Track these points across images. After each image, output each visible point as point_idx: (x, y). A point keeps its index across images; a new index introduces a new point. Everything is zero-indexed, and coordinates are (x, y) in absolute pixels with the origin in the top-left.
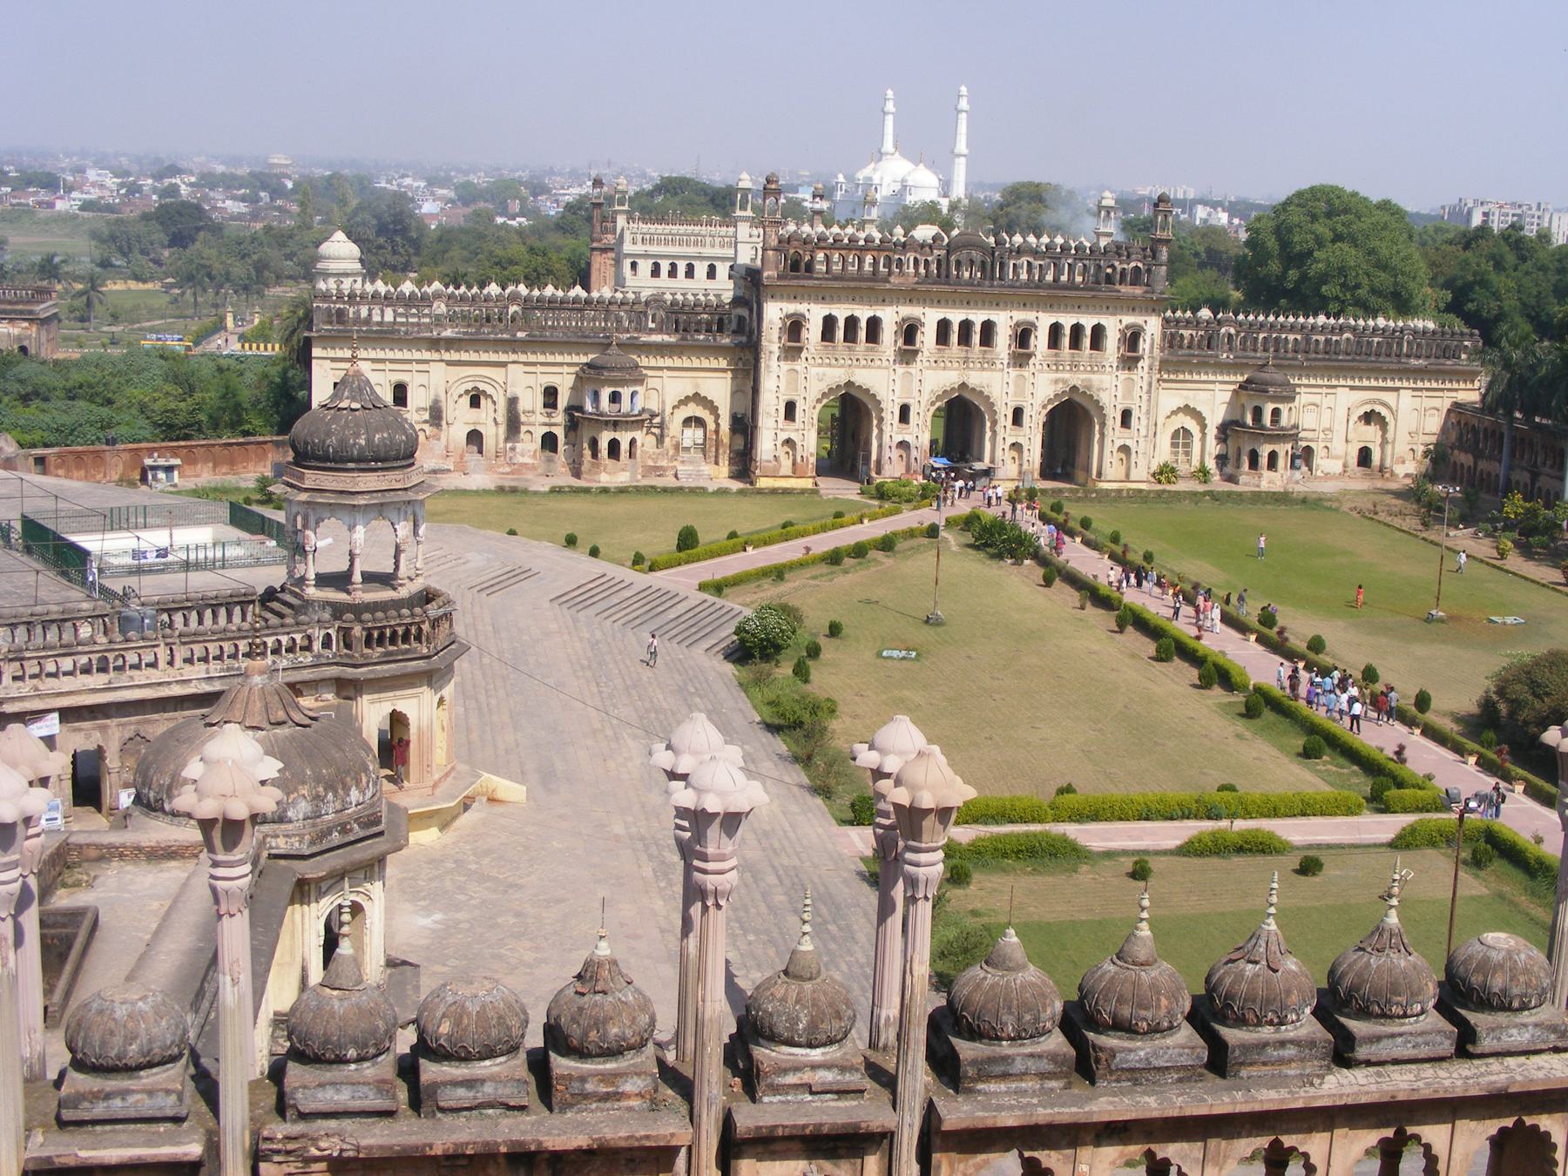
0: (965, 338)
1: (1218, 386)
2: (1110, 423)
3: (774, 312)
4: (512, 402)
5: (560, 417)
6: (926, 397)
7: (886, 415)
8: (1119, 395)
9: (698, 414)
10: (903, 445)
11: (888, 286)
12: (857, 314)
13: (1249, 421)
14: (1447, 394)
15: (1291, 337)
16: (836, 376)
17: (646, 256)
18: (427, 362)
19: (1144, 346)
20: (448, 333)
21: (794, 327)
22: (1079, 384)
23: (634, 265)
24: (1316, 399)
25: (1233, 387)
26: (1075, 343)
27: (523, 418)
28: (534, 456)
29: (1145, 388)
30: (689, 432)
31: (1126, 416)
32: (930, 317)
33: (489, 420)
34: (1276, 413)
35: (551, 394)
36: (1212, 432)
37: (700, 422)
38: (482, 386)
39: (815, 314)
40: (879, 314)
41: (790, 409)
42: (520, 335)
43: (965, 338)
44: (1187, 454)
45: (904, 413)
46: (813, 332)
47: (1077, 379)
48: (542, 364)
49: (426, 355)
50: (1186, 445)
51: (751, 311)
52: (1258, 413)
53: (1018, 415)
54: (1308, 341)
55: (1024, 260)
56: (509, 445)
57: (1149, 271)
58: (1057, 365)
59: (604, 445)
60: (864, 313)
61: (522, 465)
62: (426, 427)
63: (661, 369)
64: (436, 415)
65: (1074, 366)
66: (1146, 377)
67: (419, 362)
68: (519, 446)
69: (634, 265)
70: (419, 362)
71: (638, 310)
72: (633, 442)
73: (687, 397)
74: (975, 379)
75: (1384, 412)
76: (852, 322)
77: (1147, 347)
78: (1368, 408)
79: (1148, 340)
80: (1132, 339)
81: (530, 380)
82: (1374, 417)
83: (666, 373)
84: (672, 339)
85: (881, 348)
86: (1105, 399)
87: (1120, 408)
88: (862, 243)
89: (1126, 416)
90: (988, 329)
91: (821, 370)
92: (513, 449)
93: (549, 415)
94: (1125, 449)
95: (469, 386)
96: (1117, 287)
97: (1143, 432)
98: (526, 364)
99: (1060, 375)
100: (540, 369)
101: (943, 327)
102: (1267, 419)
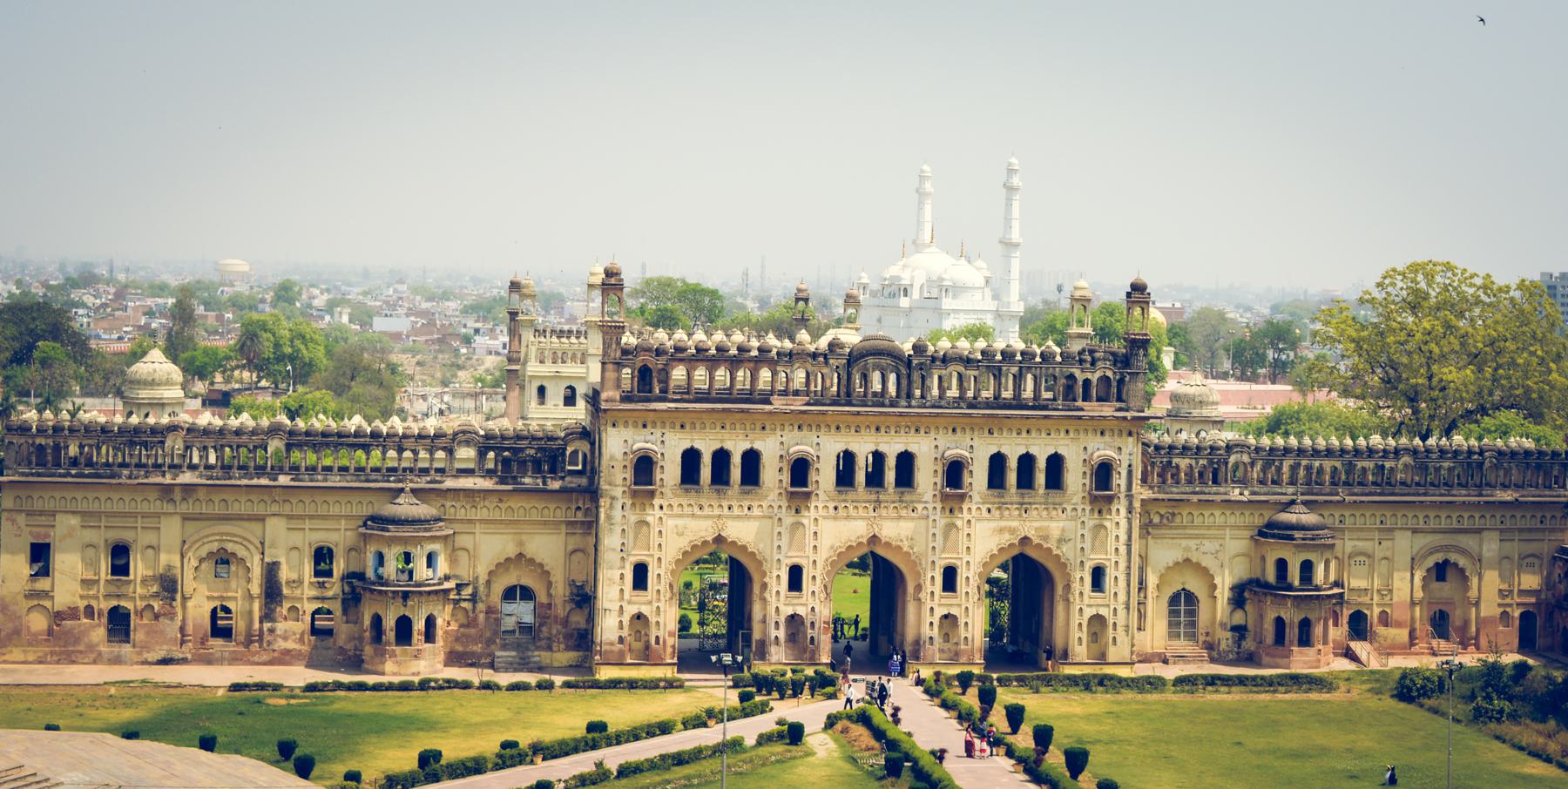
0: (875, 479)
2: (1076, 586)
3: (618, 444)
4: (271, 571)
5: (334, 587)
6: (823, 555)
7: (771, 581)
8: (1087, 545)
9: (527, 581)
10: (794, 619)
11: (767, 407)
12: (728, 446)
13: (1271, 576)
14: (1547, 536)
15: (1328, 464)
17: (557, 377)
18: (158, 516)
19: (1119, 480)
20: (187, 477)
21: (644, 467)
22: (1031, 534)
23: (542, 391)
24: (1360, 544)
25: (1247, 534)
26: (1026, 480)
27: (285, 591)
28: (301, 640)
29: (1123, 538)
30: (509, 607)
31: (1098, 575)
32: (825, 449)
34: (1307, 567)
35: (323, 556)
36: (1223, 594)
37: (527, 594)
38: (230, 547)
39: (669, 448)
40: (757, 446)
41: (640, 576)
42: (283, 480)
43: (875, 479)
44: (1193, 624)
45: (795, 578)
48: (311, 517)
49: (157, 506)
50: (1192, 613)
51: (592, 444)
52: (1282, 565)
53: (950, 579)
54: (1350, 468)
55: (954, 370)
56: (267, 625)
57: (1121, 382)
59: (389, 623)
60: (737, 448)
61: (287, 652)
63: (470, 521)
64: (169, 586)
66: (1124, 524)
67: (145, 516)
68: (281, 626)
69: (542, 391)
70: (145, 516)
71: (445, 442)
72: (430, 622)
73: (508, 560)
75: (1462, 562)
76: (721, 457)
77: (1123, 482)
78: (1439, 557)
79: (1124, 473)
80: (1103, 474)
81: (297, 538)
82: (1450, 574)
83: (478, 528)
84: (487, 484)
85: (762, 491)
86: (1068, 552)
87: (1089, 566)
88: (754, 353)
89: (1098, 575)
90: (906, 462)
91: (680, 522)
92: (272, 631)
93: (321, 585)
94: (1098, 620)
95: (215, 547)
96: (1080, 403)
97: (1122, 597)
98: (290, 517)
99: (1003, 524)
100: (307, 524)
101: (847, 461)
102: (1294, 576)
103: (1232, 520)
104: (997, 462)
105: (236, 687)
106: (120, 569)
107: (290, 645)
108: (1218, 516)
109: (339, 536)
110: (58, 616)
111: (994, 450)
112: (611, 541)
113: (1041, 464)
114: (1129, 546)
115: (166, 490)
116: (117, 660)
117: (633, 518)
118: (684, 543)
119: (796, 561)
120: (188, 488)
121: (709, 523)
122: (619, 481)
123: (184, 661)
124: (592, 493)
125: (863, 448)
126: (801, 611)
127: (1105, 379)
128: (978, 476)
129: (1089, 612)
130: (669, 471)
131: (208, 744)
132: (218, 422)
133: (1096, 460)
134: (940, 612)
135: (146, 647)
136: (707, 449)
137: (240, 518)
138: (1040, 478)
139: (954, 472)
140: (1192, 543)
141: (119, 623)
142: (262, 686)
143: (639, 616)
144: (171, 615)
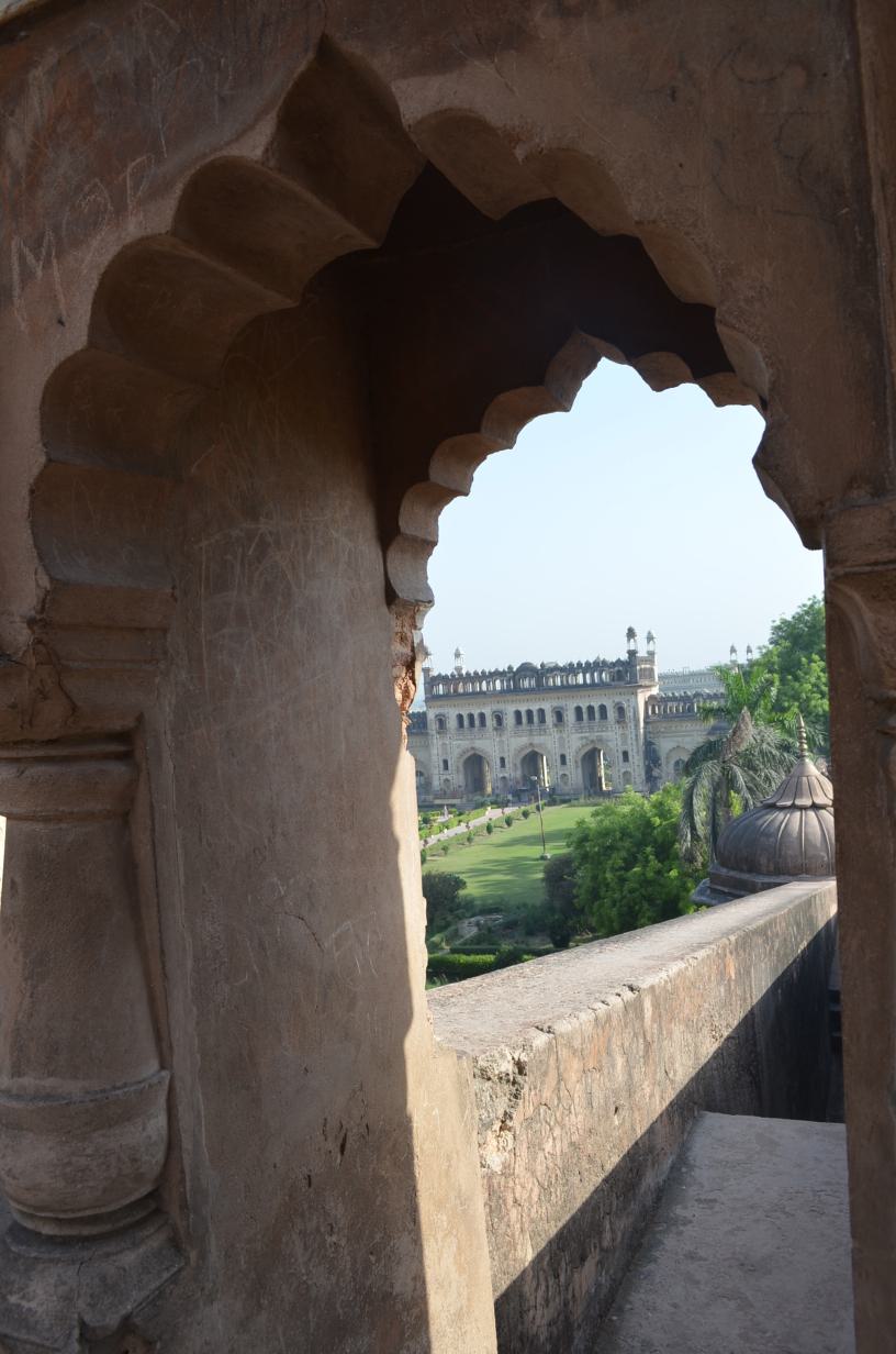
0: (530, 720)
1: (695, 733)
3: (431, 715)
6: (512, 752)
8: (619, 744)
10: (504, 778)
12: (473, 712)
16: (465, 744)
19: (629, 714)
31: (625, 754)
43: (530, 720)
45: (502, 760)
46: (452, 723)
47: (594, 736)
58: (580, 730)
65: (591, 729)
74: (537, 740)
76: (471, 716)
77: (632, 714)
80: (621, 710)
89: (625, 754)
90: (541, 712)
103: (698, 727)
104: (578, 710)
108: (688, 726)
111: (575, 705)
112: (435, 752)
113: (596, 709)
114: (637, 740)
117: (440, 743)
118: (459, 750)
119: (502, 755)
121: (467, 742)
122: (434, 728)
124: (427, 734)
125: (523, 709)
126: (506, 775)
127: (619, 671)
128: (570, 717)
129: (623, 770)
130: (452, 723)
133: (618, 704)
134: (561, 773)
136: (465, 714)
138: (597, 715)
139: (559, 716)
140: (680, 739)
143: (447, 780)
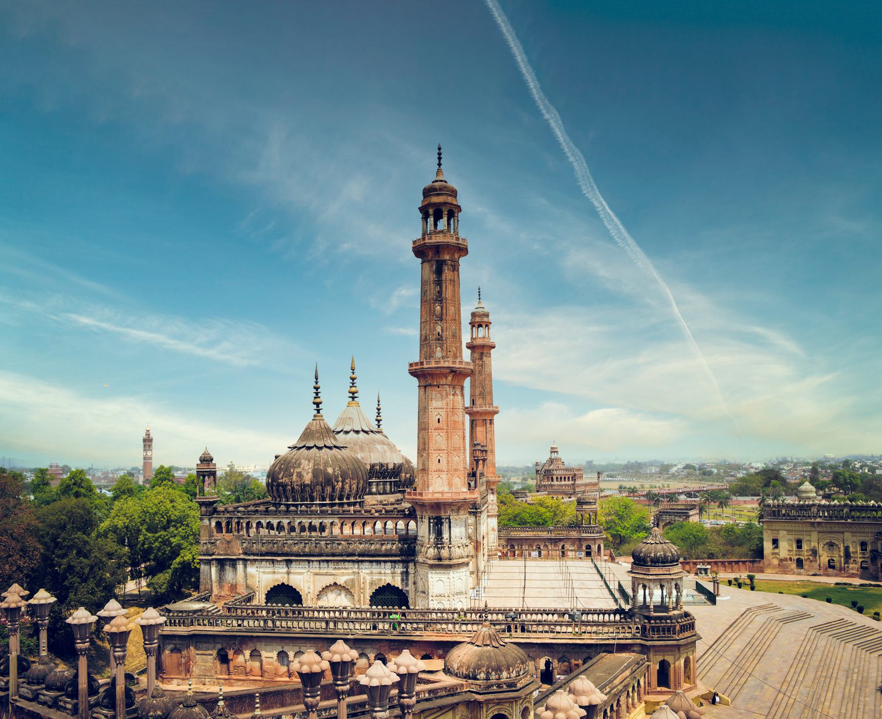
4: (847, 549)
20: (818, 520)
33: (838, 556)
35: (863, 545)
42: (849, 521)
49: (810, 528)
62: (811, 558)
64: (814, 552)
68: (851, 566)
81: (855, 539)
105: (837, 584)
106: (799, 546)
107: (854, 572)
109: (868, 538)
110: (781, 560)
115: (812, 524)
116: (799, 574)
120: (819, 523)
123: (820, 575)
131: (829, 601)
132: (827, 503)
135: (808, 570)
137: (836, 532)
141: (800, 563)
142: (845, 584)
144: (816, 561)
